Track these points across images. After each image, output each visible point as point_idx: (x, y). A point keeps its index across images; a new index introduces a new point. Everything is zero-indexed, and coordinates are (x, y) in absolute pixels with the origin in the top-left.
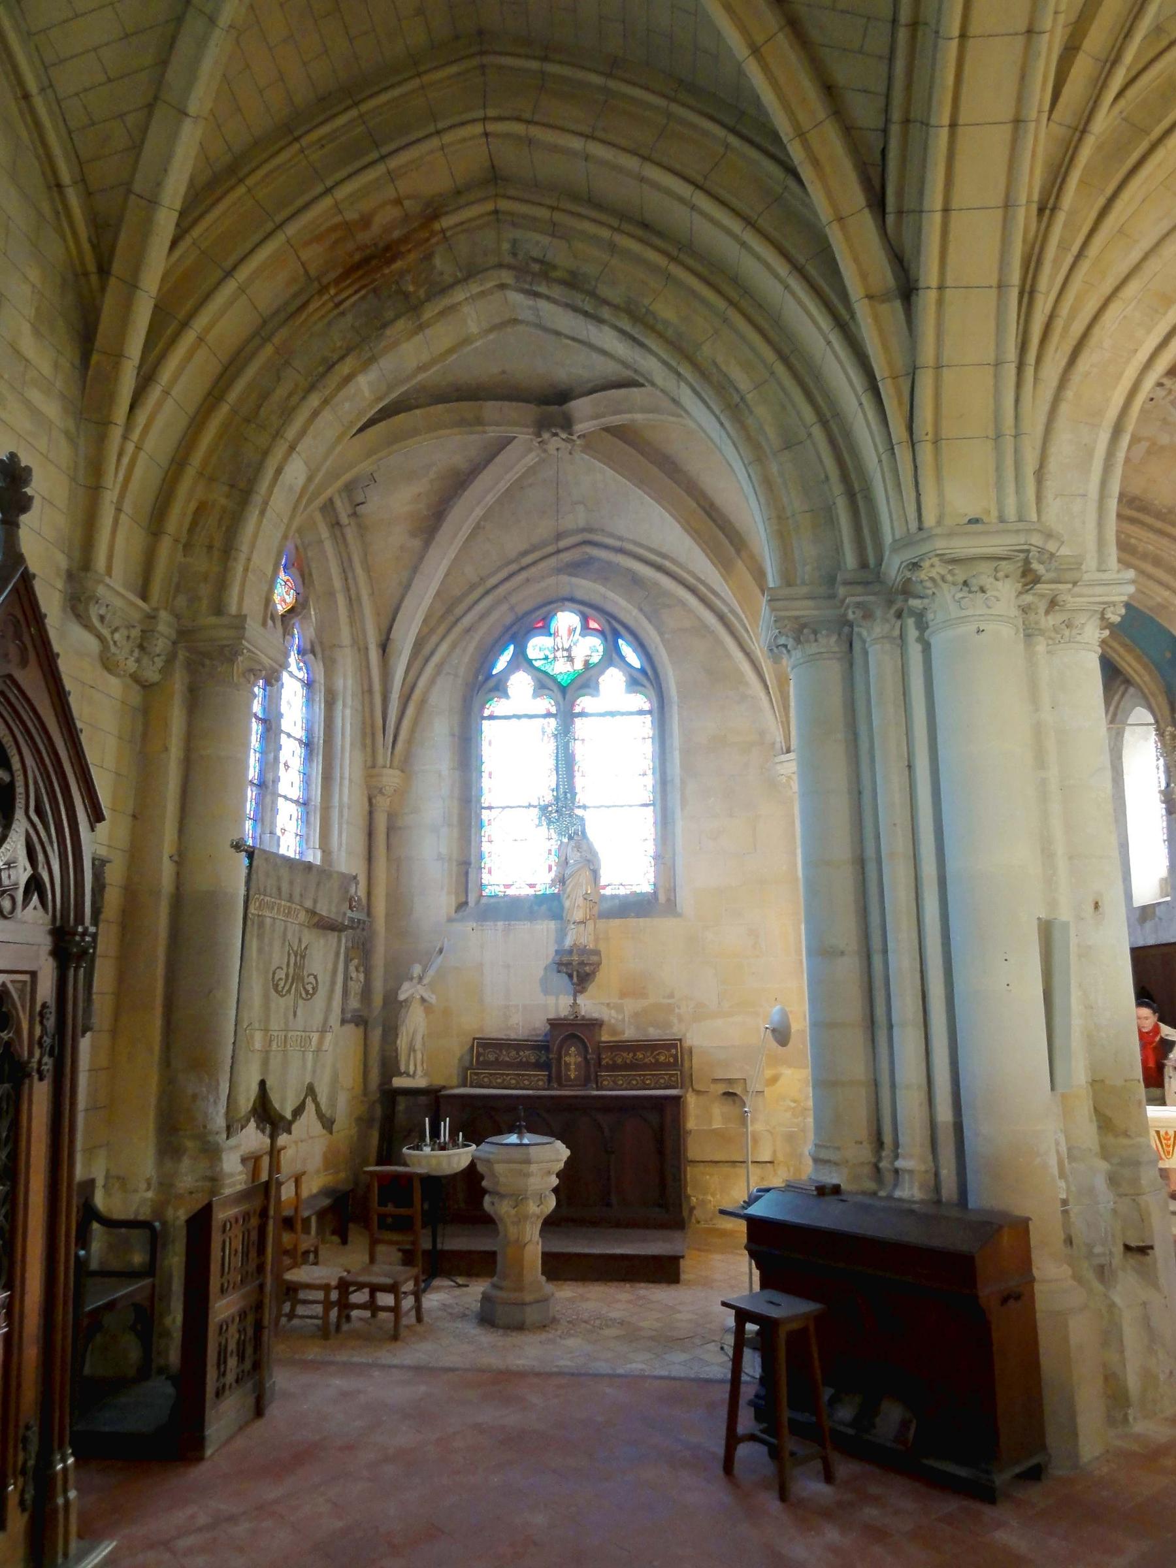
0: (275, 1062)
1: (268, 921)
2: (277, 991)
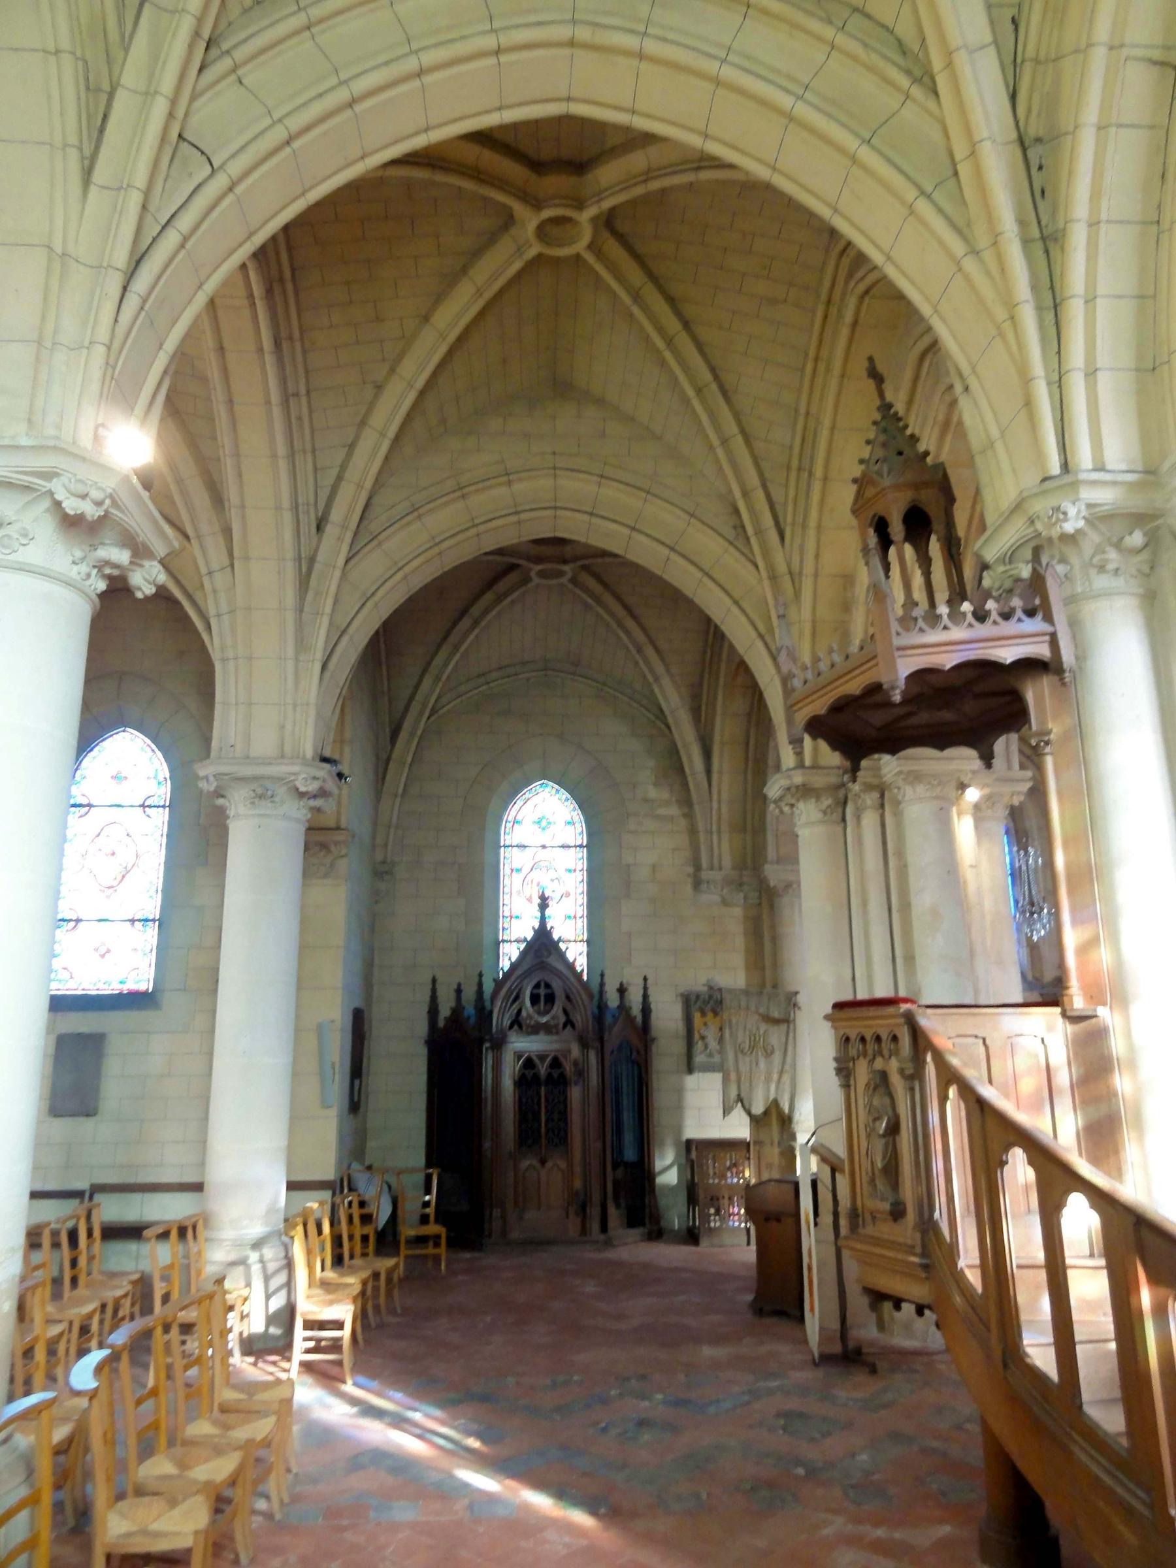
0: (745, 1086)
1: (734, 1021)
2: (742, 1052)
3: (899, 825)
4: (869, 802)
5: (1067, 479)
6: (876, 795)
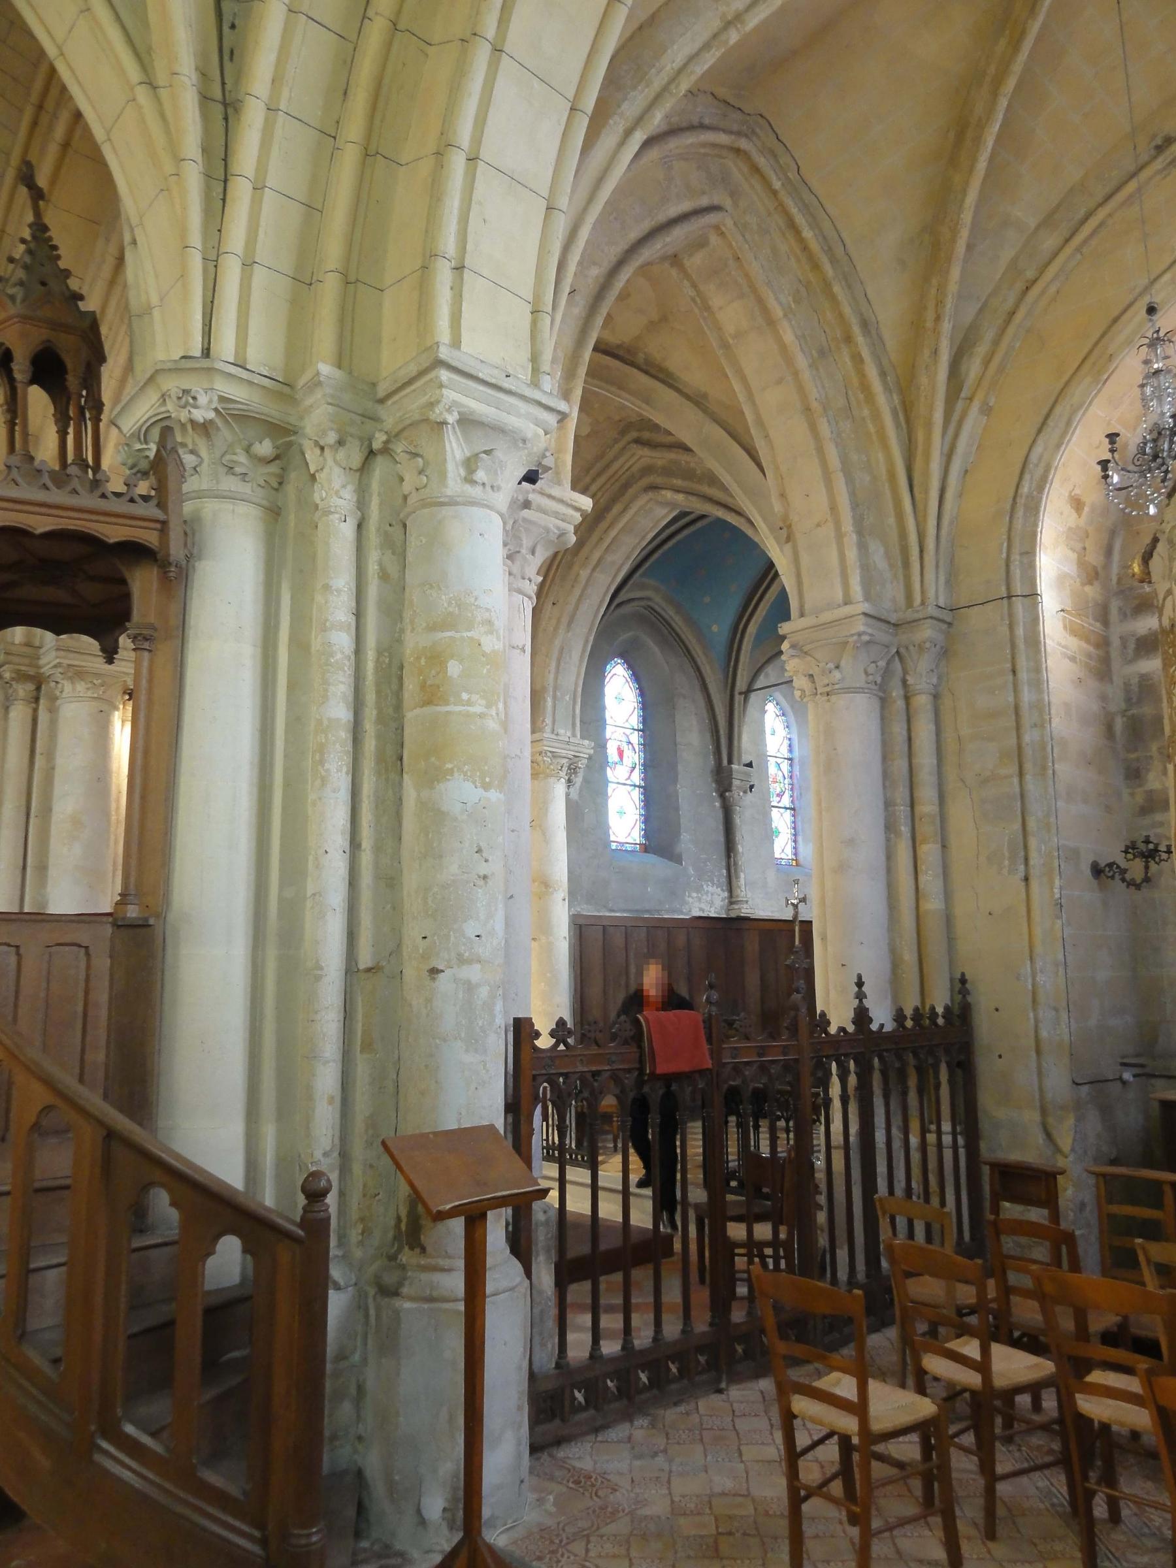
3: (53, 723)
4: (21, 693)
5: (205, 363)
6: (31, 687)
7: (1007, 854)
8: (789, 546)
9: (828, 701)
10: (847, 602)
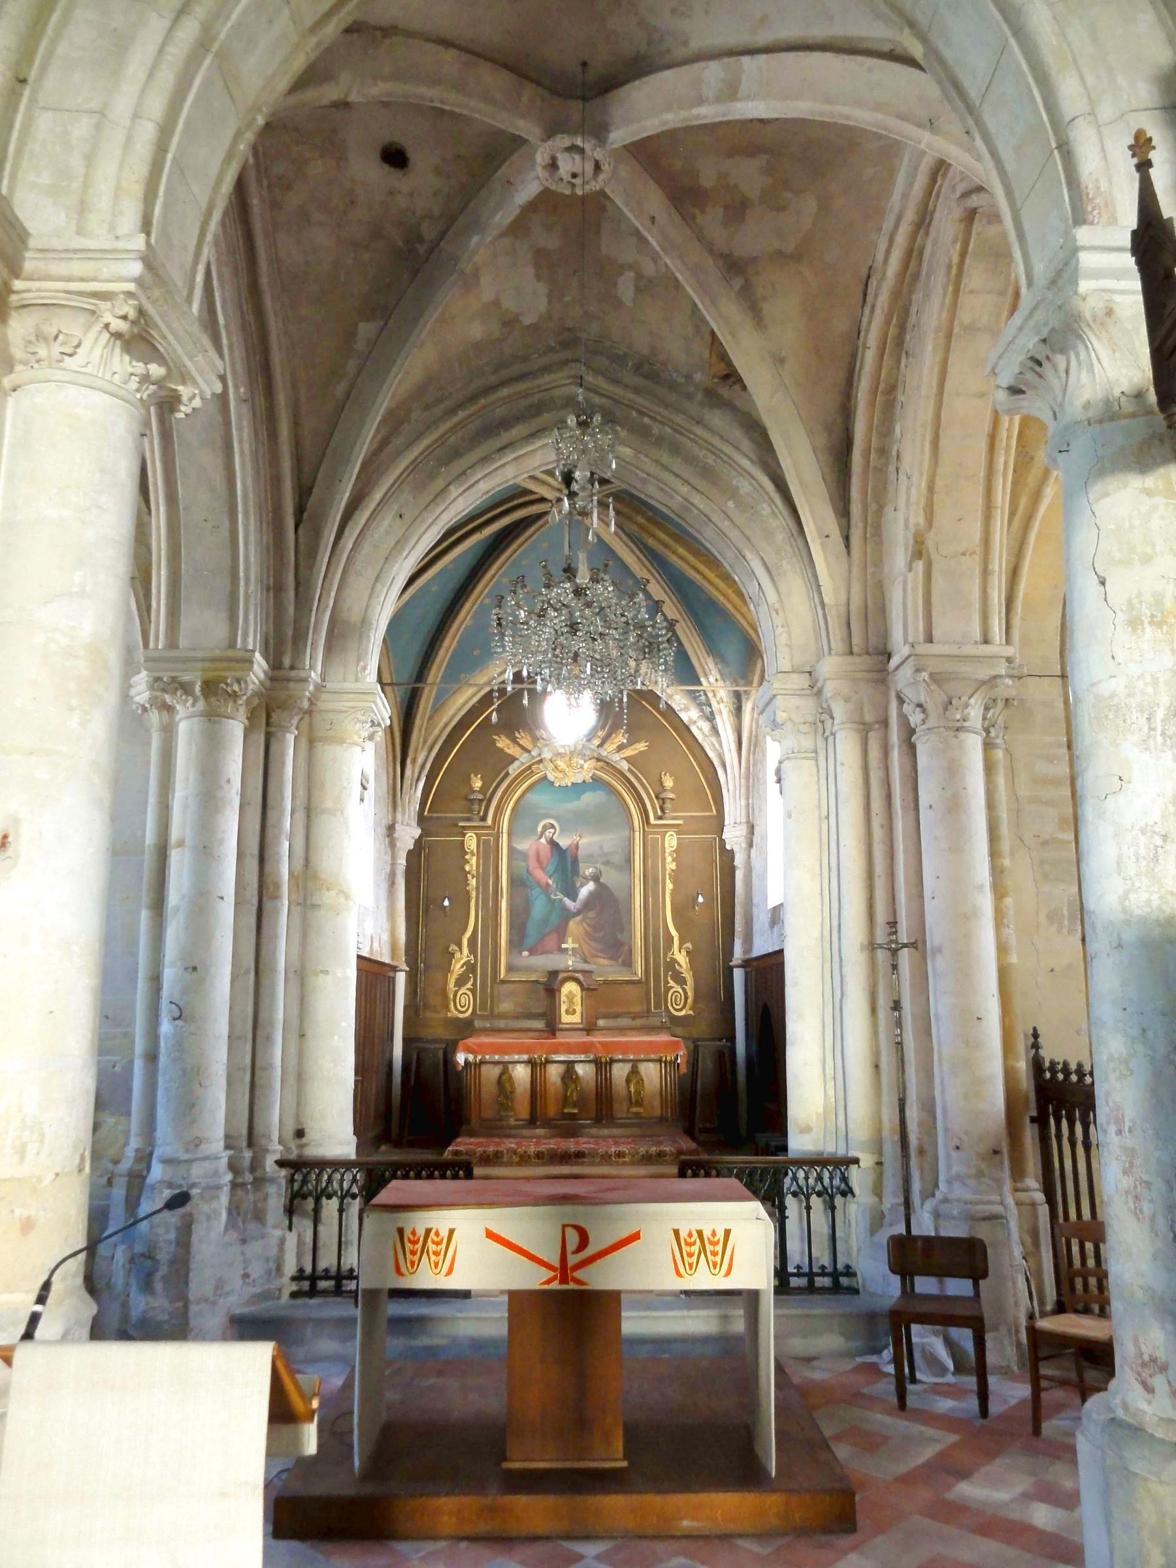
7: (1066, 913)
8: (920, 565)
9: (956, 737)
10: (986, 641)
